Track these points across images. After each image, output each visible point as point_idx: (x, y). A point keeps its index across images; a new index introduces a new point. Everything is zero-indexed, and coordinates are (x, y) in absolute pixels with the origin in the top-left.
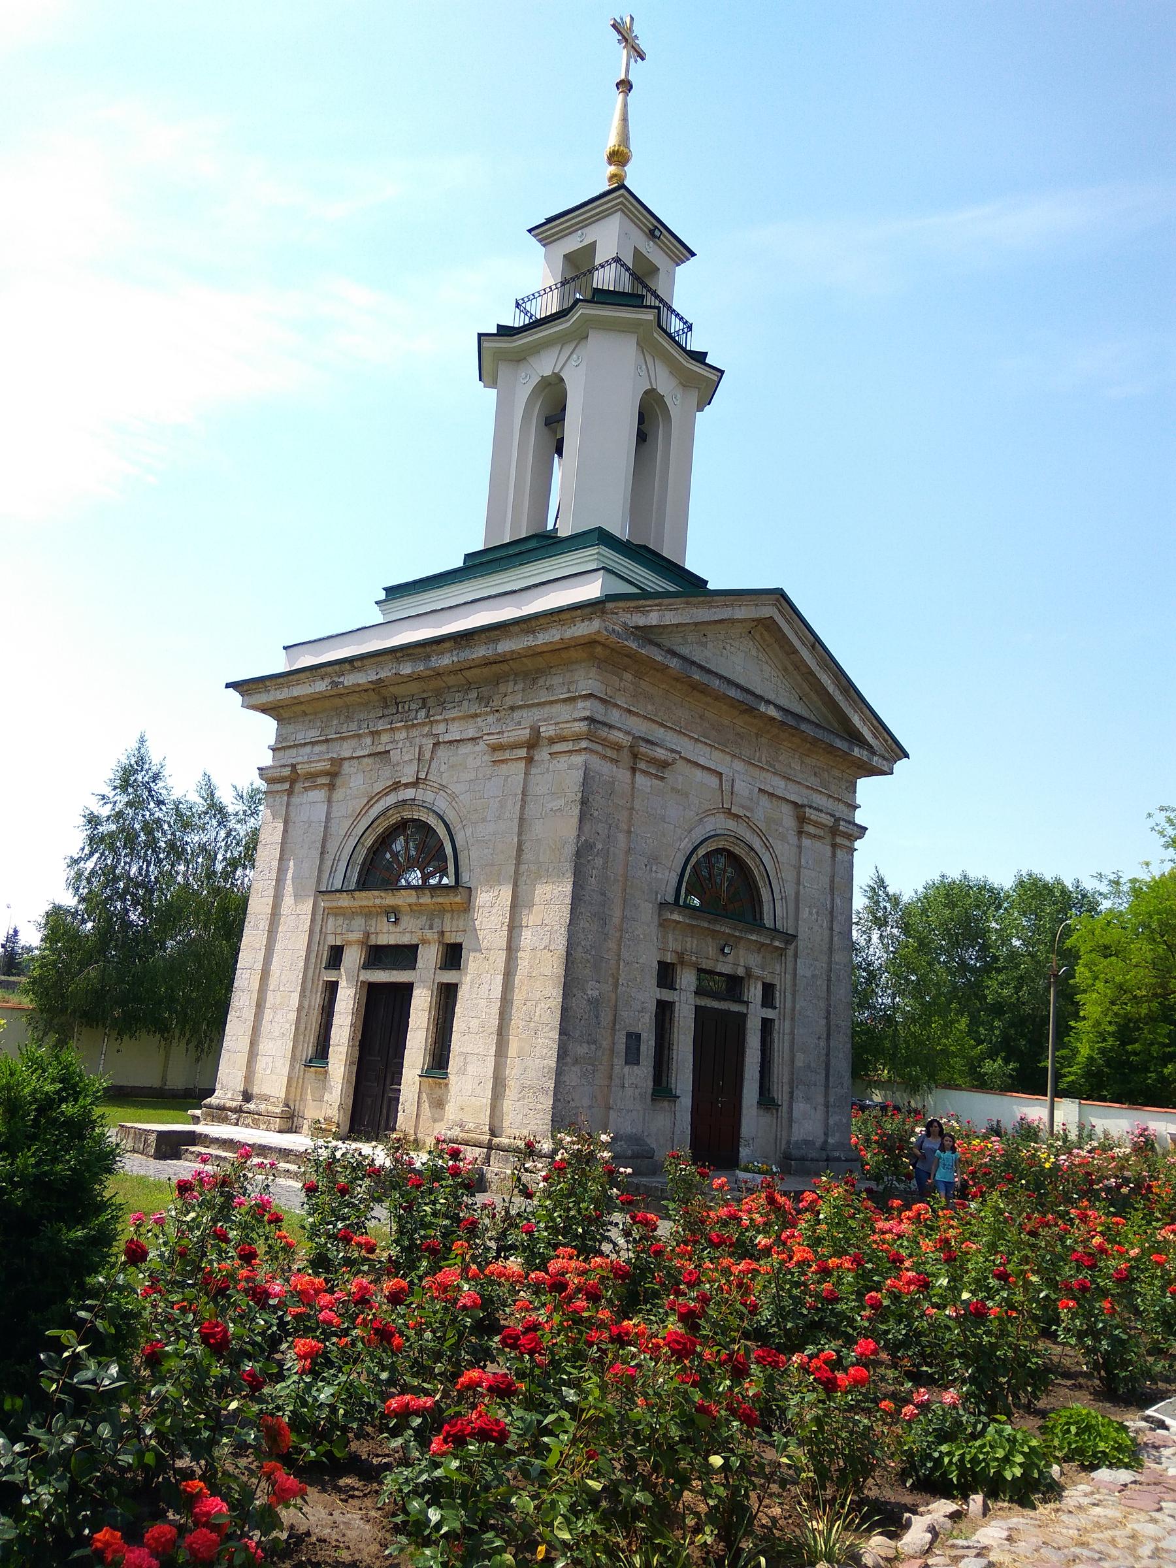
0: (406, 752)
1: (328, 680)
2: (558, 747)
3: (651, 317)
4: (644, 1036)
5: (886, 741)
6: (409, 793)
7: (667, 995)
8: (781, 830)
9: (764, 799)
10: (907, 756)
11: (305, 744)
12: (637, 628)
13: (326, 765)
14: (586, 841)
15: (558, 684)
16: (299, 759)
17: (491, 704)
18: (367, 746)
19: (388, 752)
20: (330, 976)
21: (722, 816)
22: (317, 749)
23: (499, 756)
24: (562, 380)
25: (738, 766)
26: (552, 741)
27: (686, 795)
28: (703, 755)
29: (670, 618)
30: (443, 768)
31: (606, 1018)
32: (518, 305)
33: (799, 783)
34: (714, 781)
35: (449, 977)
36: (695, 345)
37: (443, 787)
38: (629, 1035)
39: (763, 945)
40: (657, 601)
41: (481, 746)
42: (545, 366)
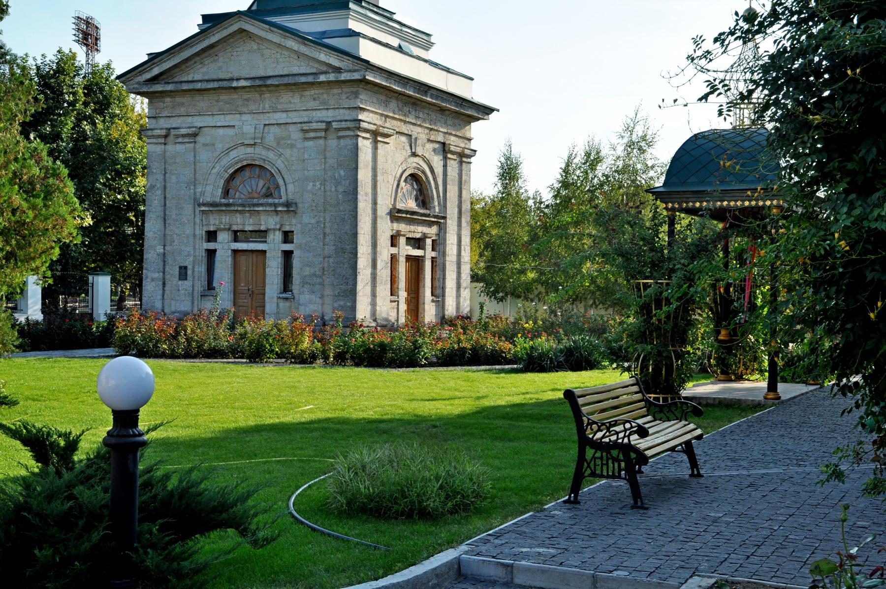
4: (190, 267)
7: (211, 246)
8: (289, 142)
21: (242, 147)
27: (213, 145)
28: (219, 120)
31: (170, 260)
34: (231, 132)
38: (181, 268)
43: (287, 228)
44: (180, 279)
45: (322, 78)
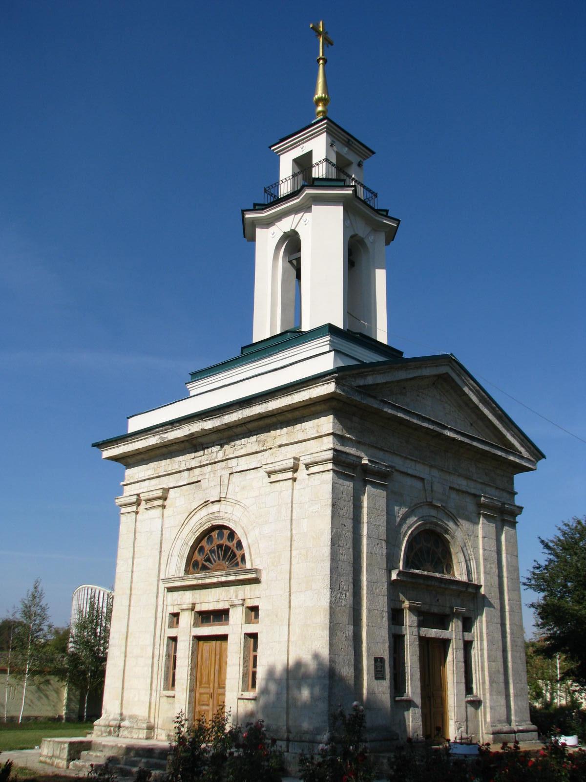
0: (212, 480)
1: (157, 437)
2: (313, 469)
3: (350, 192)
5: (530, 448)
6: (216, 508)
9: (453, 495)
10: (544, 457)
11: (144, 480)
12: (359, 387)
13: (159, 493)
14: (337, 531)
15: (310, 427)
16: (142, 490)
17: (266, 444)
18: (185, 478)
19: (200, 481)
20: (172, 632)
22: (153, 482)
23: (274, 478)
24: (297, 233)
25: (435, 472)
26: (308, 466)
29: (380, 379)
30: (237, 489)
32: (266, 191)
33: (475, 481)
34: (419, 484)
35: (251, 629)
36: (379, 204)
37: (237, 503)
38: (376, 659)
39: (461, 592)
40: (371, 369)
41: (262, 473)
42: (285, 225)
43: (467, 615)
44: (377, 678)
45: (511, 458)
